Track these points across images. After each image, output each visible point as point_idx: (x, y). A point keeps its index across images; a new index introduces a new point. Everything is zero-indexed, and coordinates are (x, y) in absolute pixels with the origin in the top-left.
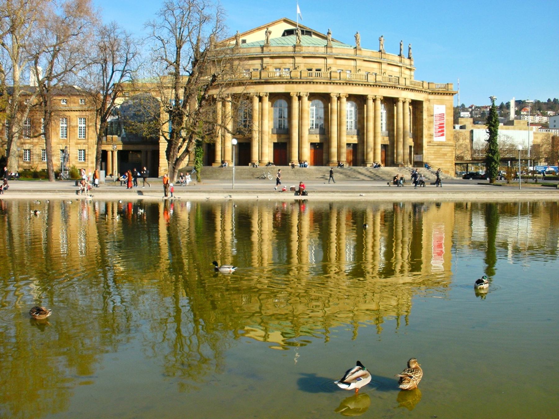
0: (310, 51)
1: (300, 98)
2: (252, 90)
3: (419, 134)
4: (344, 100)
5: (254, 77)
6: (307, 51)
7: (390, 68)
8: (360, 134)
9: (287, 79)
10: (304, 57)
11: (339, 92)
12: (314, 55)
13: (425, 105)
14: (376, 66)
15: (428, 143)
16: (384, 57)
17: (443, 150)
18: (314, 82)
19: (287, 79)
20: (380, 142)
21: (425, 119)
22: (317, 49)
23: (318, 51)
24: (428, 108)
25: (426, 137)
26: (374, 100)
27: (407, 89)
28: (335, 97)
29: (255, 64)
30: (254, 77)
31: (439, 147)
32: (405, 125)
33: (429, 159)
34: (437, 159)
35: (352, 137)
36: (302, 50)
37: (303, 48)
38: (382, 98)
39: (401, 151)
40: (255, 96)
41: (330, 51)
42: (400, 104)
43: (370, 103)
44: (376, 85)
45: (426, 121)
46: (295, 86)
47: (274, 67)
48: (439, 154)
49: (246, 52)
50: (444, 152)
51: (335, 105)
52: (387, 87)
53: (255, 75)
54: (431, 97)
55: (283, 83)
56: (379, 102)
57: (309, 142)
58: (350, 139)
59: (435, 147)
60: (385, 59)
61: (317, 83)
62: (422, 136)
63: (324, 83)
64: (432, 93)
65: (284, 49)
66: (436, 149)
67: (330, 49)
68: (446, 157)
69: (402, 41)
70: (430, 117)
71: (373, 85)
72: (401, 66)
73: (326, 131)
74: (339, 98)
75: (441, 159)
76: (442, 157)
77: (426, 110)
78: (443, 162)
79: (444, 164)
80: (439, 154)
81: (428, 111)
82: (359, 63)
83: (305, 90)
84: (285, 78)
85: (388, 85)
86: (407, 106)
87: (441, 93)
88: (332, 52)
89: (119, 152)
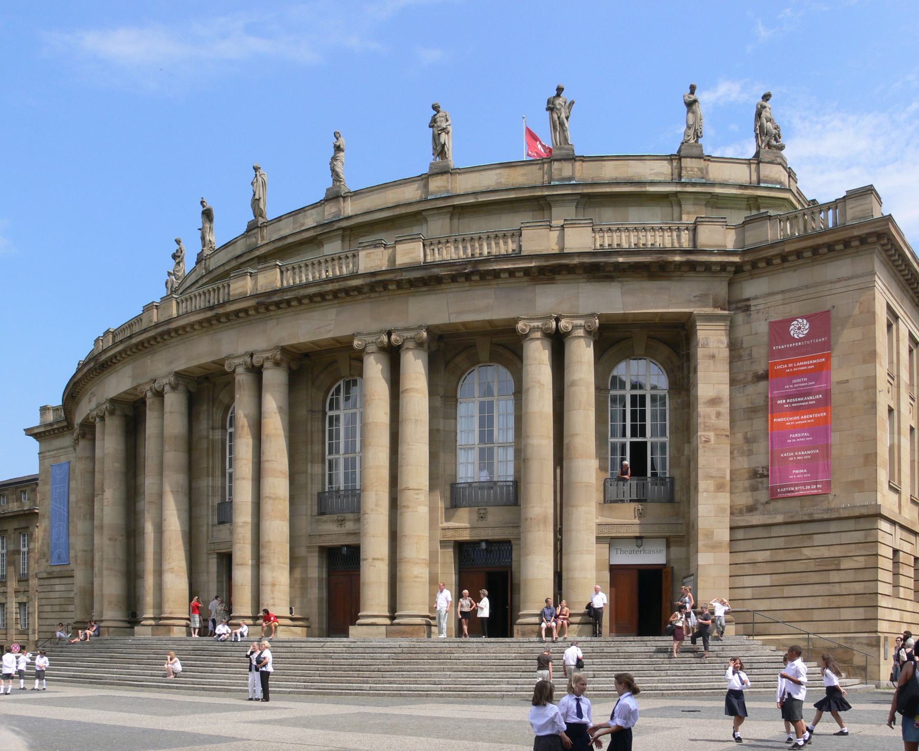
11: (251, 348)
17: (818, 540)
25: (720, 487)
31: (796, 530)
34: (787, 591)
48: (796, 566)
50: (825, 552)
54: (751, 288)
59: (775, 531)
64: (754, 265)
66: (781, 543)
68: (835, 577)
70: (751, 389)
75: (806, 590)
76: (815, 578)
78: (819, 602)
79: (828, 614)
80: (796, 566)
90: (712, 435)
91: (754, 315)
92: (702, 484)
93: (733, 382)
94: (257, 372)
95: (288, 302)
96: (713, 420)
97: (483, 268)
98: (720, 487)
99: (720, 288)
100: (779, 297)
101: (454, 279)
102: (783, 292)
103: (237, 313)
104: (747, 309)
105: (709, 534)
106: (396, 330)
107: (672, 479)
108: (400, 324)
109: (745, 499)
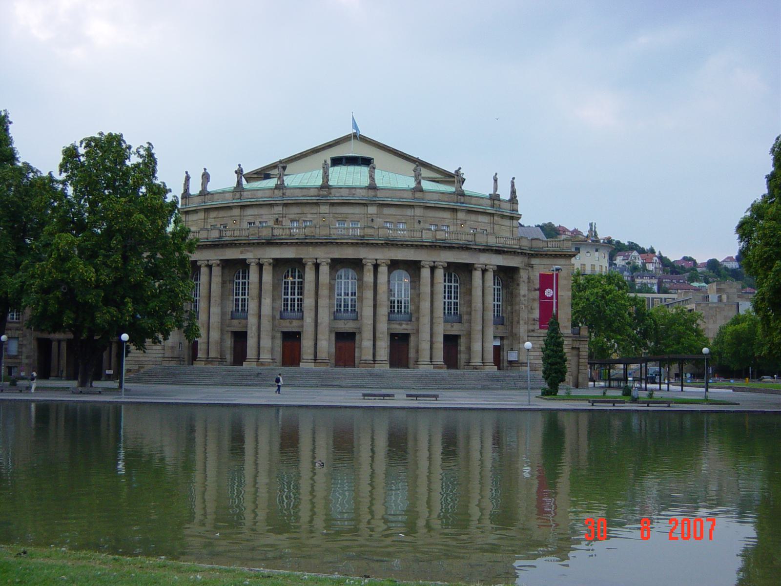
0: (343, 194)
1: (317, 266)
2: (250, 255)
3: (516, 319)
4: (383, 270)
5: (252, 235)
6: (337, 194)
7: (473, 217)
8: (413, 319)
9: (297, 239)
10: (333, 204)
11: (377, 258)
12: (347, 201)
13: (523, 274)
14: (447, 215)
15: (529, 331)
16: (462, 201)
18: (337, 243)
19: (297, 239)
20: (440, 331)
21: (524, 296)
22: (353, 191)
23: (354, 194)
24: (529, 278)
25: (525, 323)
26: (433, 269)
27: (488, 250)
28: (369, 264)
29: (262, 215)
30: (252, 235)
32: (486, 305)
33: (532, 358)
35: (401, 324)
36: (330, 193)
37: (333, 191)
38: (446, 265)
39: (477, 347)
40: (252, 264)
41: (373, 194)
42: (477, 275)
43: (426, 273)
44: (435, 246)
45: (526, 298)
46: (310, 249)
47: (289, 218)
49: (250, 197)
51: (369, 277)
52: (453, 247)
53: (253, 232)
54: (535, 261)
55: (292, 244)
56: (440, 273)
57: (331, 331)
58: (398, 327)
60: (463, 203)
61: (342, 243)
62: (518, 322)
63: (352, 243)
65: (305, 192)
67: (373, 191)
69: (496, 174)
71: (430, 246)
72: (493, 214)
73: (359, 315)
74: (376, 267)
77: (526, 281)
81: (529, 282)
82: (419, 212)
83: (324, 255)
84: (296, 237)
85: (454, 245)
86: (490, 276)
87: (551, 255)
88: (376, 196)
89: (69, 342)
90: (523, 306)
91: (535, 270)
92: (521, 322)
93: (528, 290)
94: (376, 267)
95: (397, 245)
96: (524, 302)
97: (468, 246)
98: (525, 323)
99: (526, 259)
100: (543, 266)
101: (458, 248)
102: (544, 265)
103: (372, 244)
104: (532, 267)
105: (523, 338)
106: (436, 261)
107: (503, 317)
108: (438, 260)
109: (531, 327)
